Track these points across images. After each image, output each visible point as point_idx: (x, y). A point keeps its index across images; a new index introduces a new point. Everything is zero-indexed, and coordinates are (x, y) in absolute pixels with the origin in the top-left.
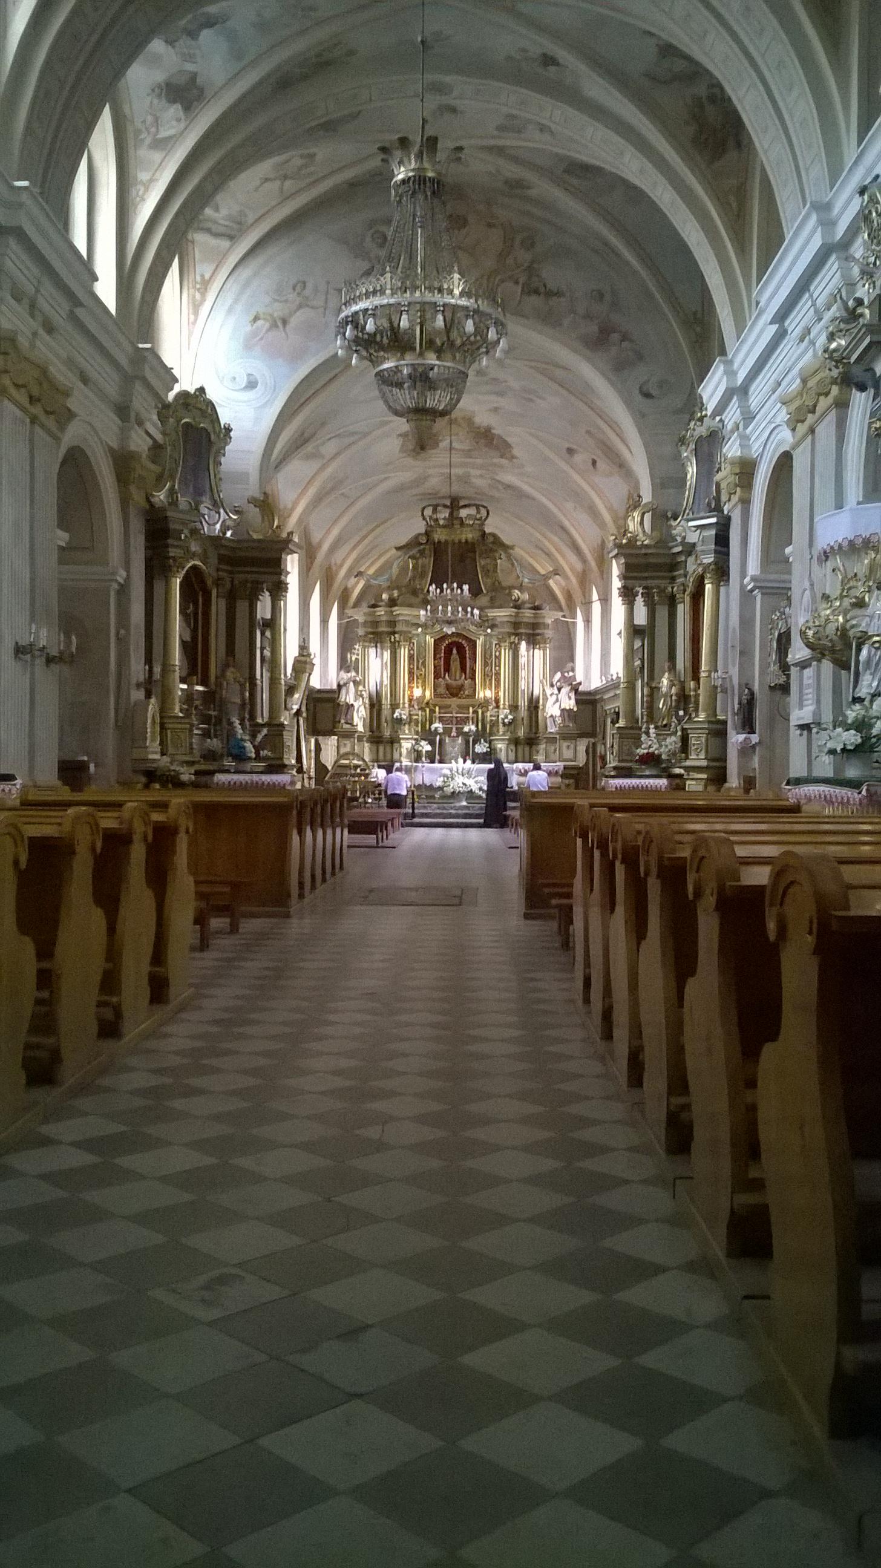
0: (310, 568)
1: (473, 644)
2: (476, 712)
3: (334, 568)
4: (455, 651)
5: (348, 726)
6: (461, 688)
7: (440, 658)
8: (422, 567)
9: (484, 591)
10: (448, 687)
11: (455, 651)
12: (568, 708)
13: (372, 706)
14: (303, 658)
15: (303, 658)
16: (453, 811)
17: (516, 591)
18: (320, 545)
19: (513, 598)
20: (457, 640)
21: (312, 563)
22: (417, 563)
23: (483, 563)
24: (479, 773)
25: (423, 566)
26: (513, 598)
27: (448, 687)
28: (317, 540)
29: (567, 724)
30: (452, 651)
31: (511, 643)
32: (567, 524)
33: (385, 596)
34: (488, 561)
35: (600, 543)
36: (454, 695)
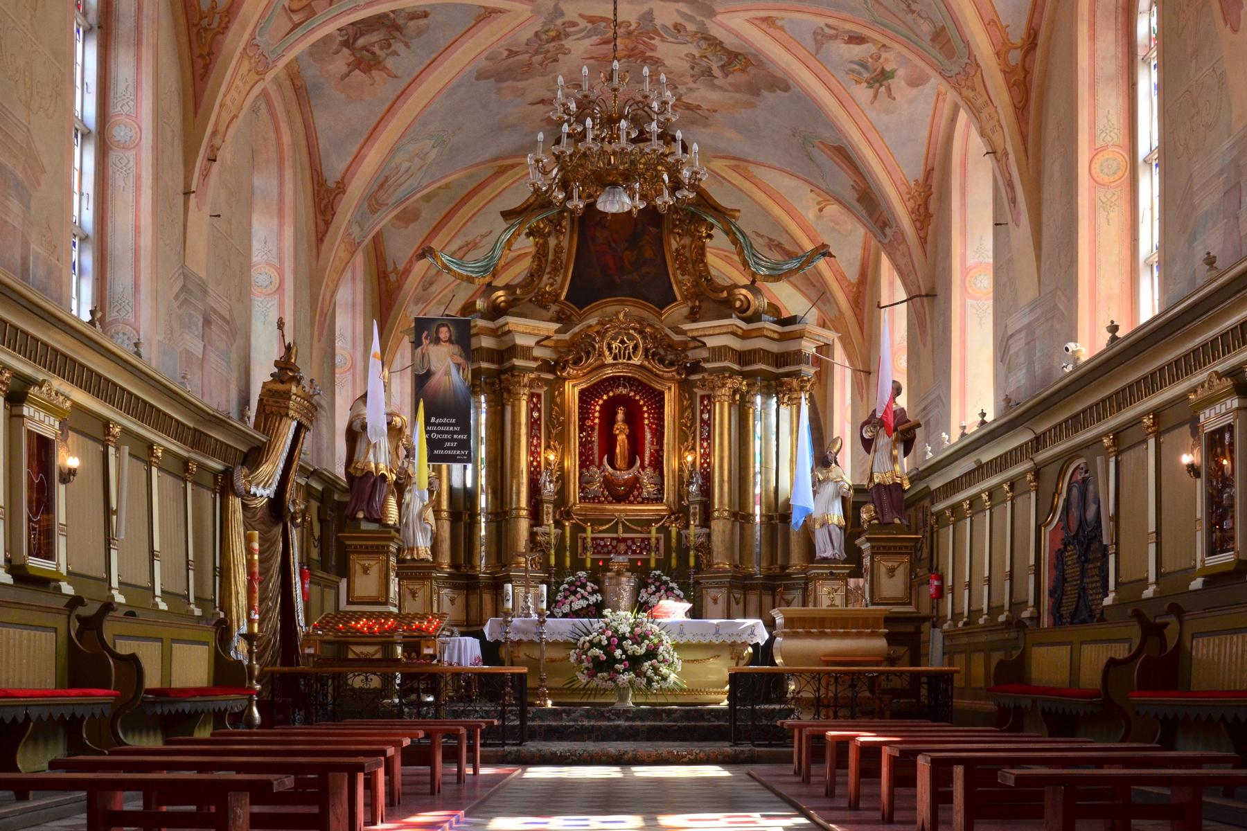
0: (326, 232)
1: (657, 400)
2: (664, 530)
3: (393, 278)
4: (620, 416)
5: (374, 527)
6: (635, 483)
7: (592, 428)
8: (556, 252)
9: (679, 297)
10: (608, 483)
11: (620, 416)
12: (889, 481)
13: (455, 517)
14: (279, 387)
15: (279, 387)
16: (622, 723)
17: (744, 291)
18: (341, 187)
19: (738, 304)
20: (624, 392)
21: (328, 224)
22: (546, 243)
23: (674, 245)
24: (718, 564)
25: (558, 249)
26: (738, 304)
27: (608, 483)
28: (338, 177)
29: (887, 519)
30: (616, 413)
31: (735, 392)
32: (855, 135)
33: (480, 304)
34: (686, 241)
35: (920, 177)
36: (620, 499)
